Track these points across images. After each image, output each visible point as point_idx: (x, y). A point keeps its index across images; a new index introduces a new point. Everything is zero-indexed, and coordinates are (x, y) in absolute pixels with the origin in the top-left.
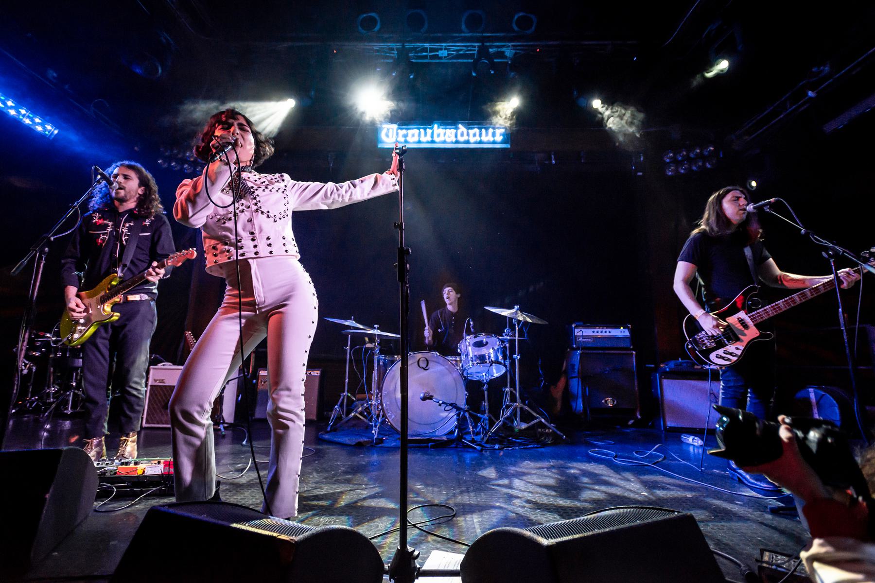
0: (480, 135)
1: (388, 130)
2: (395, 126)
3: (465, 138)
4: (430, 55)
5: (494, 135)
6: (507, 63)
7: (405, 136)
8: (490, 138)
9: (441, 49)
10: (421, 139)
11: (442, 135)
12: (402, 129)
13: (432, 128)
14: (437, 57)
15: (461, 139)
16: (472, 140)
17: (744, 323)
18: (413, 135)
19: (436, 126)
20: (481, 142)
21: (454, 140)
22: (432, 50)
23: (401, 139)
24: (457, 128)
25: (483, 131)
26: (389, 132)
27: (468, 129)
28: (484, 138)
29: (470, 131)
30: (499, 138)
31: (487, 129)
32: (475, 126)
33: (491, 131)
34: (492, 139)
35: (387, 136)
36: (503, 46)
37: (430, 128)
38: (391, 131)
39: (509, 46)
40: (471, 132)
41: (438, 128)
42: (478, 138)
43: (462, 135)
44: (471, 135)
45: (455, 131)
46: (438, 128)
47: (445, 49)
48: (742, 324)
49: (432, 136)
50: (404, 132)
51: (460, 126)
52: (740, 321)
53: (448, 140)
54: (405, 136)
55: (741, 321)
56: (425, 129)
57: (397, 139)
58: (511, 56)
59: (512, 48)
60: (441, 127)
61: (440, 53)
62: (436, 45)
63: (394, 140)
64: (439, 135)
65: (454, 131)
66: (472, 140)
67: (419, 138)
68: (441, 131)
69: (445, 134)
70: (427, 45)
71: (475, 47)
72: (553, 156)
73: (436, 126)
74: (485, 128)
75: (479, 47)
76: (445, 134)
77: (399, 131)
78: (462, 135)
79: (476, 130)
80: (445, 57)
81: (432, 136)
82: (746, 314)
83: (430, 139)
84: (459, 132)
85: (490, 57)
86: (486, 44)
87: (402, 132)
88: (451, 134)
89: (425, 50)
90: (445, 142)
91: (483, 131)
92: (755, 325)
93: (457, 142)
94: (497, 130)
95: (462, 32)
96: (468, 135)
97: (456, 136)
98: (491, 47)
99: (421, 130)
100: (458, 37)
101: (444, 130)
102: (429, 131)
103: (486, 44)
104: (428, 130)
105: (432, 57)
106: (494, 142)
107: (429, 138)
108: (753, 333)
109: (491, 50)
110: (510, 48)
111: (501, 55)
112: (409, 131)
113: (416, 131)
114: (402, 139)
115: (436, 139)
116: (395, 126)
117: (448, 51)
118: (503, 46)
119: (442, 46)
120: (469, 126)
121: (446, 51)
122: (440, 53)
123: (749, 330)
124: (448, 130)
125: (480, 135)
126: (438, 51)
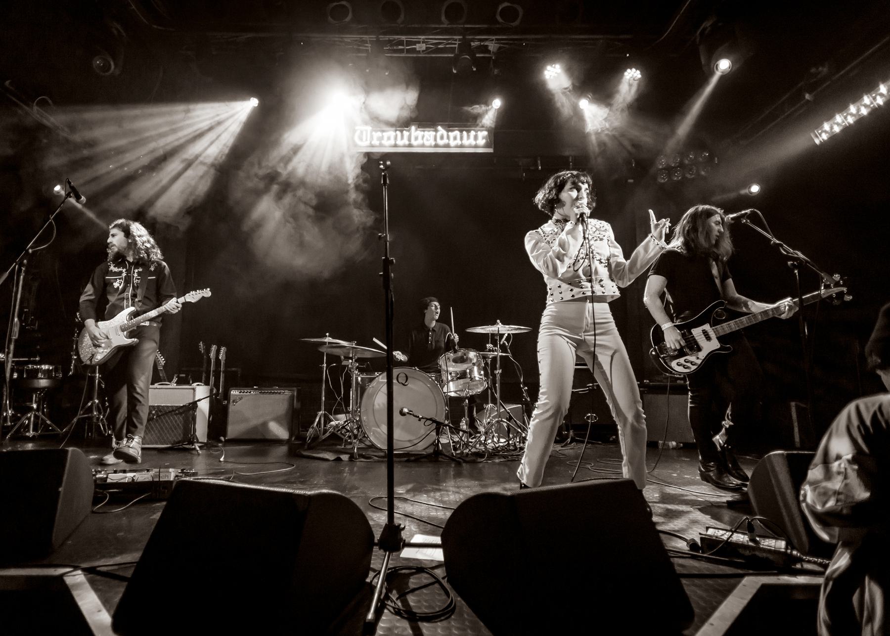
0: (461, 138)
1: (362, 132)
2: (369, 128)
3: (445, 141)
4: (407, 49)
5: (476, 138)
6: (491, 57)
7: (381, 139)
8: (472, 141)
9: (419, 42)
10: (397, 143)
11: (420, 138)
12: (376, 131)
13: (409, 131)
14: (414, 51)
15: (441, 142)
16: (453, 143)
17: (708, 335)
18: (389, 138)
19: (413, 128)
20: (462, 146)
21: (433, 143)
22: (409, 43)
24: (436, 131)
25: (465, 133)
26: (362, 134)
27: (448, 131)
28: (466, 142)
29: (450, 133)
30: (481, 142)
31: (468, 132)
32: (456, 128)
33: (473, 133)
34: (473, 143)
35: (361, 139)
36: (487, 40)
38: (364, 133)
39: (493, 40)
40: (451, 134)
41: (416, 130)
42: (458, 142)
43: (442, 138)
45: (434, 133)
46: (416, 130)
47: (423, 42)
48: (705, 335)
49: (409, 140)
50: (379, 134)
51: (439, 128)
52: (704, 333)
53: (427, 143)
54: (381, 139)
55: (705, 333)
56: (402, 131)
57: (371, 143)
58: (494, 51)
59: (496, 42)
60: (418, 129)
61: (418, 47)
62: (414, 38)
63: (368, 143)
64: (416, 138)
65: (432, 133)
66: (453, 143)
67: (396, 142)
69: (423, 137)
70: (403, 38)
71: (456, 40)
72: (539, 162)
73: (413, 128)
74: (466, 131)
75: (460, 40)
76: (423, 137)
77: (374, 133)
78: (442, 138)
79: (457, 133)
80: (423, 51)
81: (409, 140)
82: (711, 327)
83: (407, 143)
84: (439, 134)
85: (472, 52)
86: (467, 37)
88: (430, 137)
89: (401, 43)
90: (423, 146)
91: (465, 133)
92: (718, 338)
93: (436, 146)
94: (479, 132)
95: (443, 23)
96: (448, 138)
97: (435, 140)
98: (473, 40)
99: (398, 133)
100: (436, 29)
101: (423, 133)
102: (406, 133)
103: (467, 37)
104: (404, 132)
105: (408, 51)
106: (476, 146)
108: (715, 345)
109: (472, 44)
110: (493, 42)
111: (485, 49)
112: (384, 134)
115: (414, 143)
117: (426, 45)
118: (487, 40)
119: (420, 39)
120: (449, 128)
121: (424, 44)
122: (418, 47)
123: (711, 341)
124: (426, 132)
125: (461, 138)
126: (415, 45)
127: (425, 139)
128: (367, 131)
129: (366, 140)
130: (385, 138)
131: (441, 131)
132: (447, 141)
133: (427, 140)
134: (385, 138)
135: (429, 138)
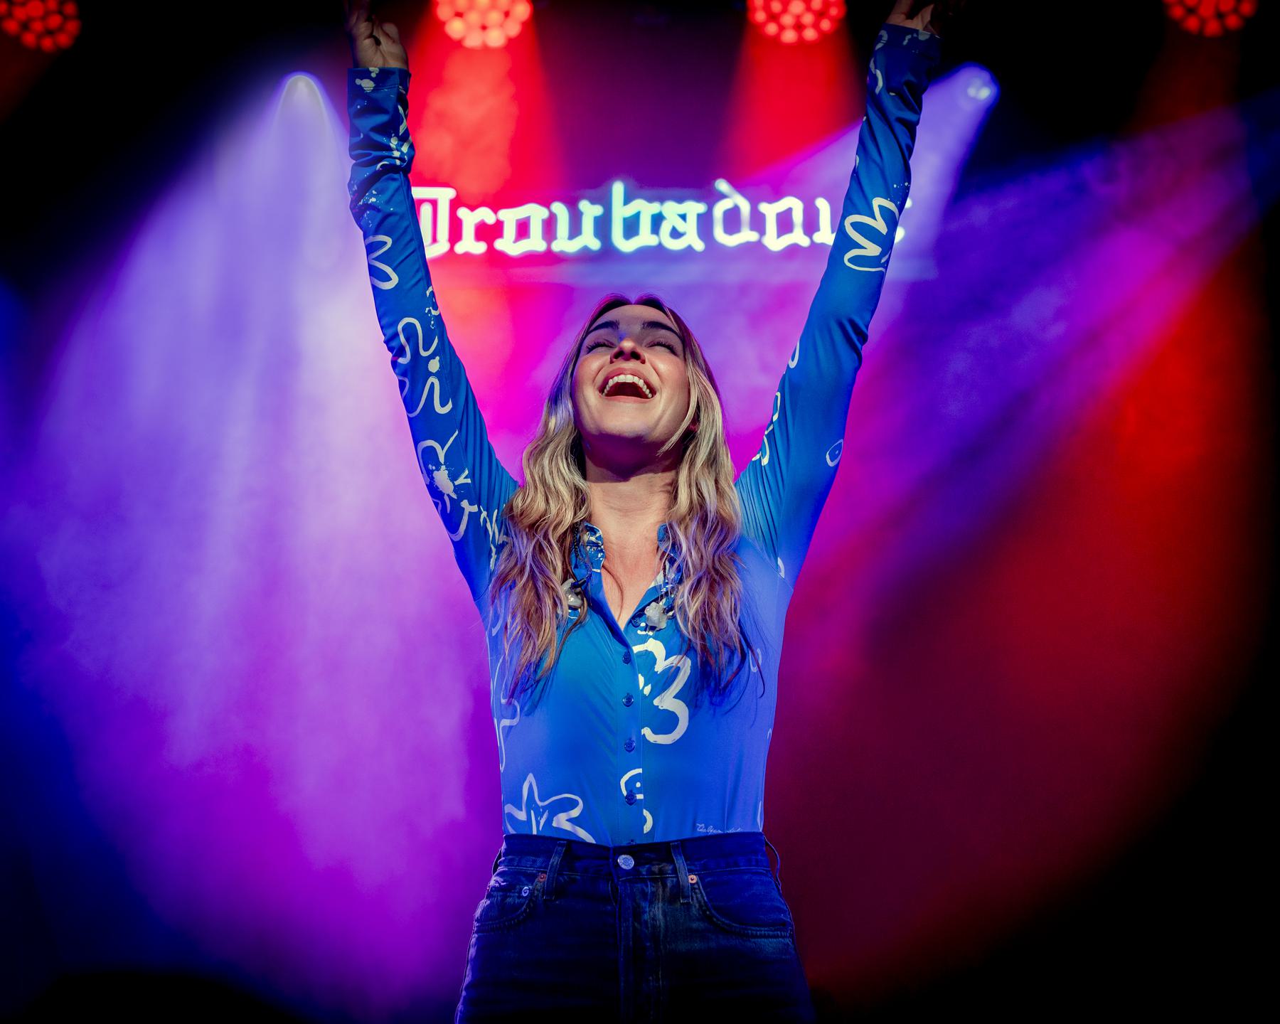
3: (747, 235)
10: (557, 246)
11: (645, 224)
18: (523, 229)
19: (618, 189)
21: (699, 246)
23: (470, 245)
24: (712, 197)
29: (764, 207)
37: (594, 201)
38: (426, 211)
40: (770, 211)
42: (798, 237)
44: (771, 225)
45: (701, 208)
46: (628, 200)
49: (603, 227)
51: (722, 185)
54: (488, 233)
64: (631, 227)
65: (694, 208)
66: (774, 242)
68: (645, 209)
69: (657, 220)
73: (618, 189)
76: (657, 220)
77: (463, 213)
79: (792, 203)
81: (603, 227)
83: (595, 245)
84: (720, 208)
87: (470, 219)
90: (657, 254)
96: (758, 222)
99: (559, 209)
101: (655, 208)
102: (590, 211)
104: (584, 205)
107: (589, 240)
113: (535, 213)
114: (480, 248)
115: (625, 246)
116: (445, 195)
124: (671, 209)
127: (665, 228)
128: (434, 203)
129: (434, 240)
130: (510, 230)
131: (723, 196)
132: (752, 236)
133: (675, 234)
134: (510, 230)
135: (681, 226)
